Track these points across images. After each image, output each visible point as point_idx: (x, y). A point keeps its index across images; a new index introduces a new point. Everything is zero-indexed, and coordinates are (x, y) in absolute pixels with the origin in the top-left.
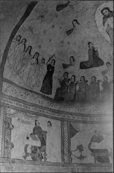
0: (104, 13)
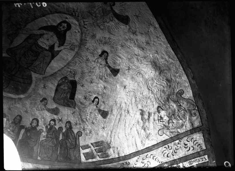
0: (61, 25)
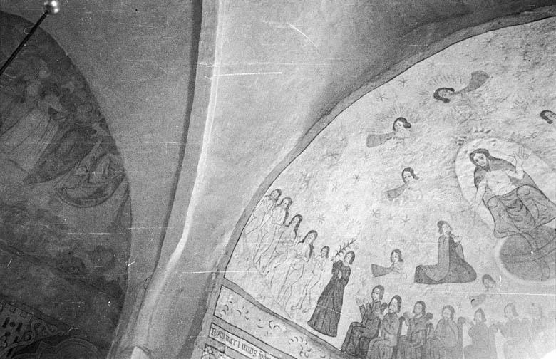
0: (477, 161)
